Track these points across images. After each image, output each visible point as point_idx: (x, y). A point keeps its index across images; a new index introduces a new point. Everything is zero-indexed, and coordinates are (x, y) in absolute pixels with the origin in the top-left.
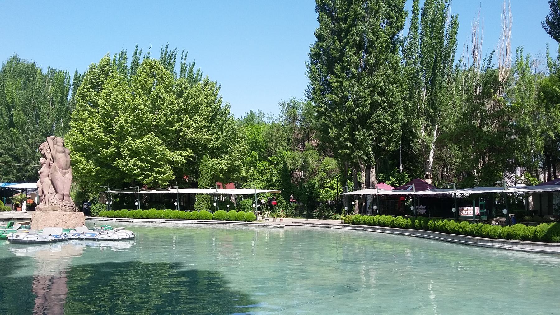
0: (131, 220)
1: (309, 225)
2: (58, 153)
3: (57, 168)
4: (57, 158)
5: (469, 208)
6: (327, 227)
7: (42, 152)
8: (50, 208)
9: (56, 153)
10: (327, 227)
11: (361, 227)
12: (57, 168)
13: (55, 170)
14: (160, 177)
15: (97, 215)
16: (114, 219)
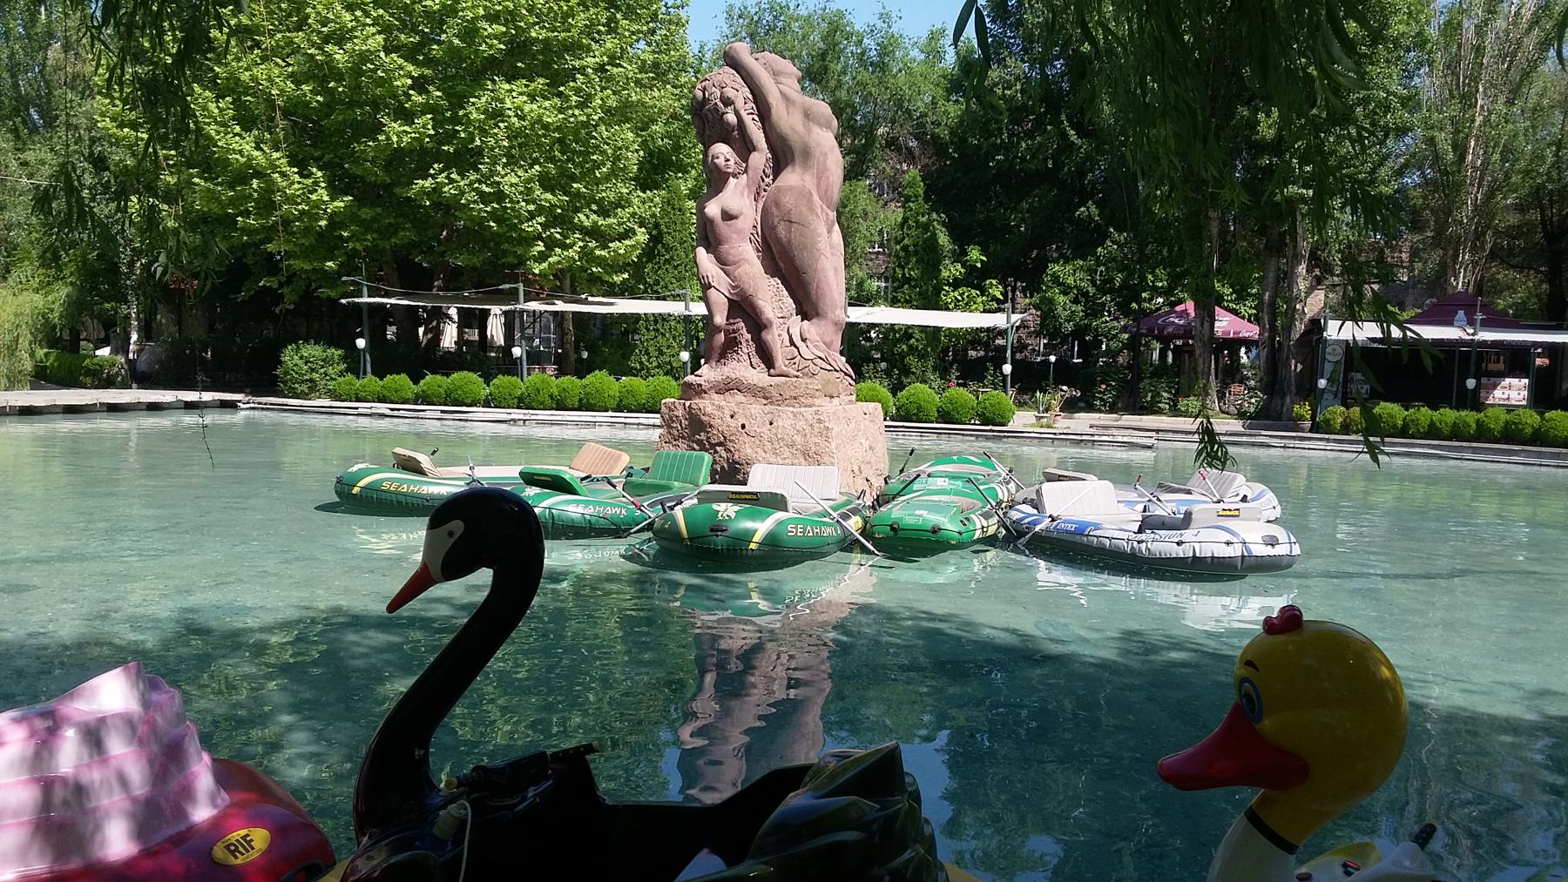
0: (517, 414)
1: (1170, 436)
2: (816, 129)
3: (816, 198)
4: (817, 152)
5: (1515, 381)
6: (1253, 445)
7: (731, 118)
8: (815, 384)
9: (809, 131)
10: (1253, 445)
11: (1421, 446)
12: (816, 198)
13: (812, 210)
14: (598, 252)
15: (313, 389)
16: (433, 411)
